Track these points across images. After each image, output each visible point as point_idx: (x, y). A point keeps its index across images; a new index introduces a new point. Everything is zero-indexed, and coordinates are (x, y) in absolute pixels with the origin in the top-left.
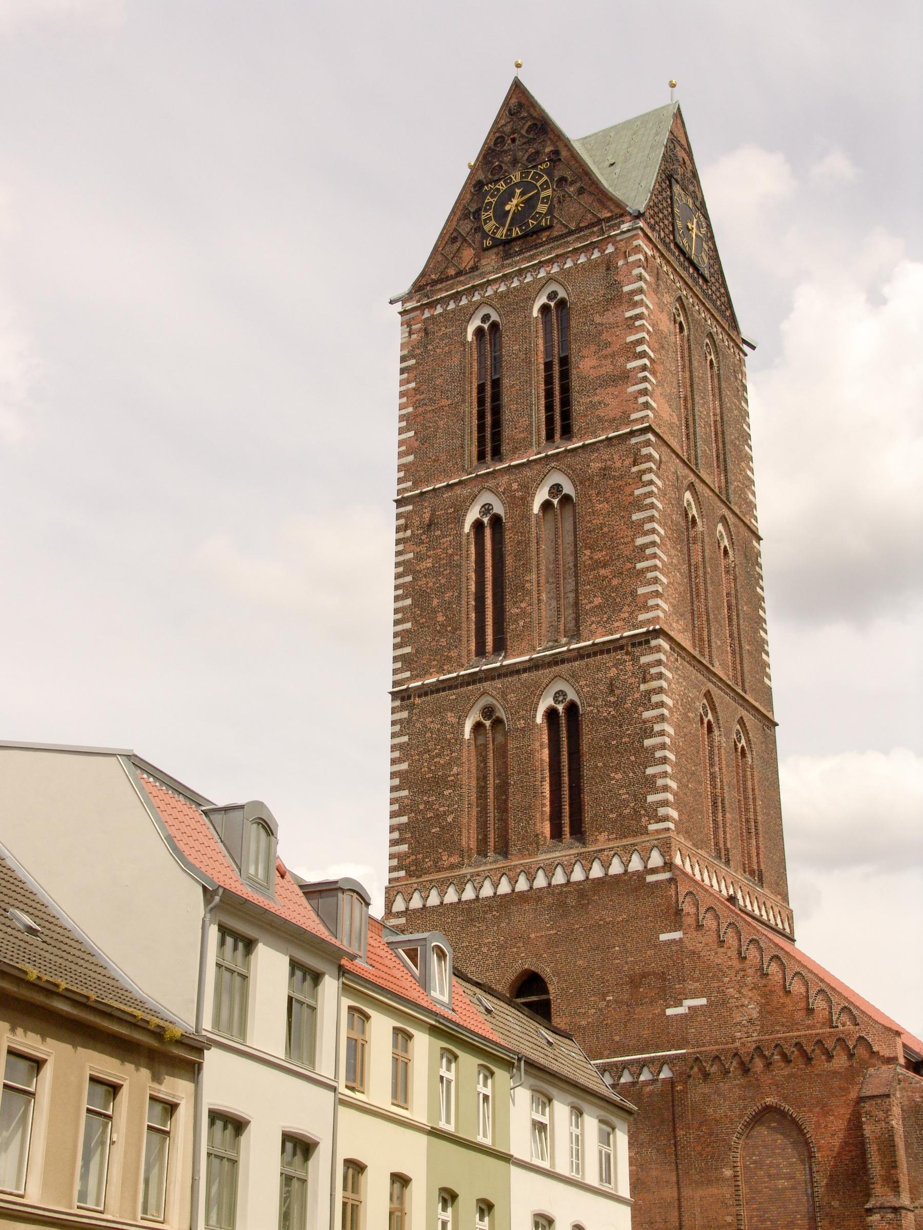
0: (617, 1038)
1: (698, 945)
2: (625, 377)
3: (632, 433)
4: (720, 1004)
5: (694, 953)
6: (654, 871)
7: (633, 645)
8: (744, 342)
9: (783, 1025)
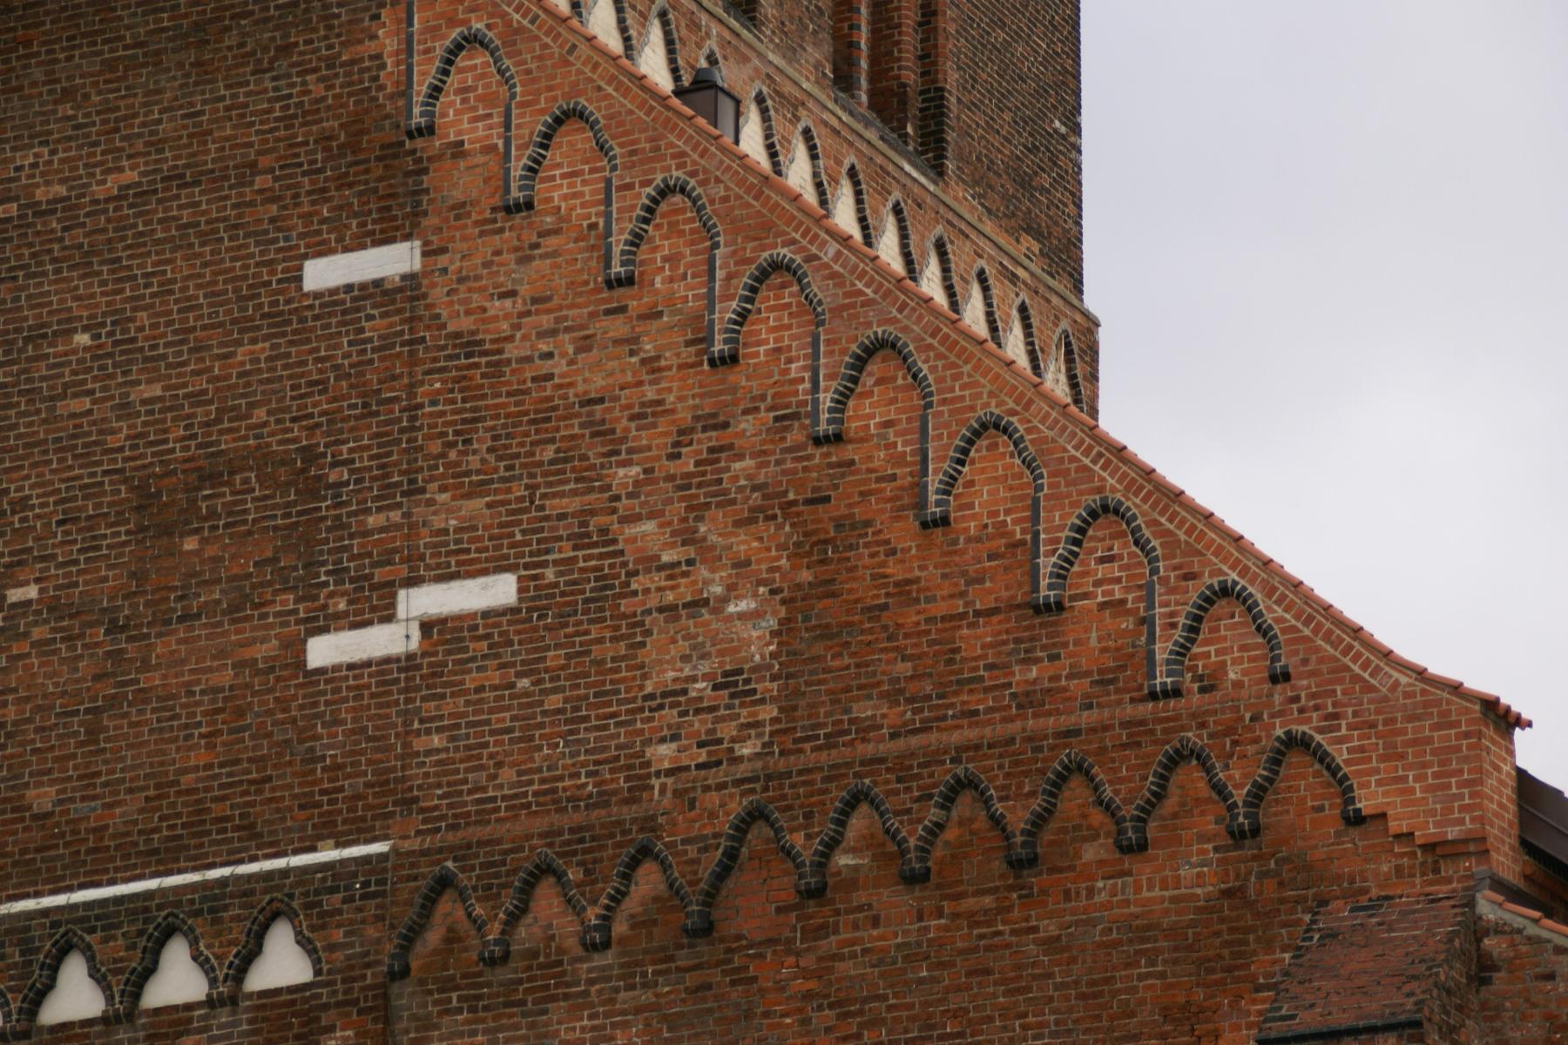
0: (42, 797)
1: (496, 307)
5: (469, 345)
9: (892, 697)
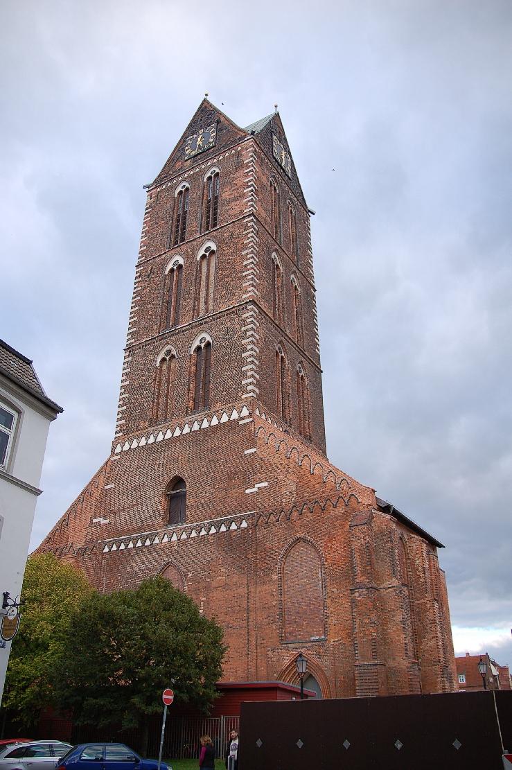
2: (243, 196)
3: (244, 218)
4: (275, 485)
6: (243, 418)
7: (239, 310)
8: (309, 211)
